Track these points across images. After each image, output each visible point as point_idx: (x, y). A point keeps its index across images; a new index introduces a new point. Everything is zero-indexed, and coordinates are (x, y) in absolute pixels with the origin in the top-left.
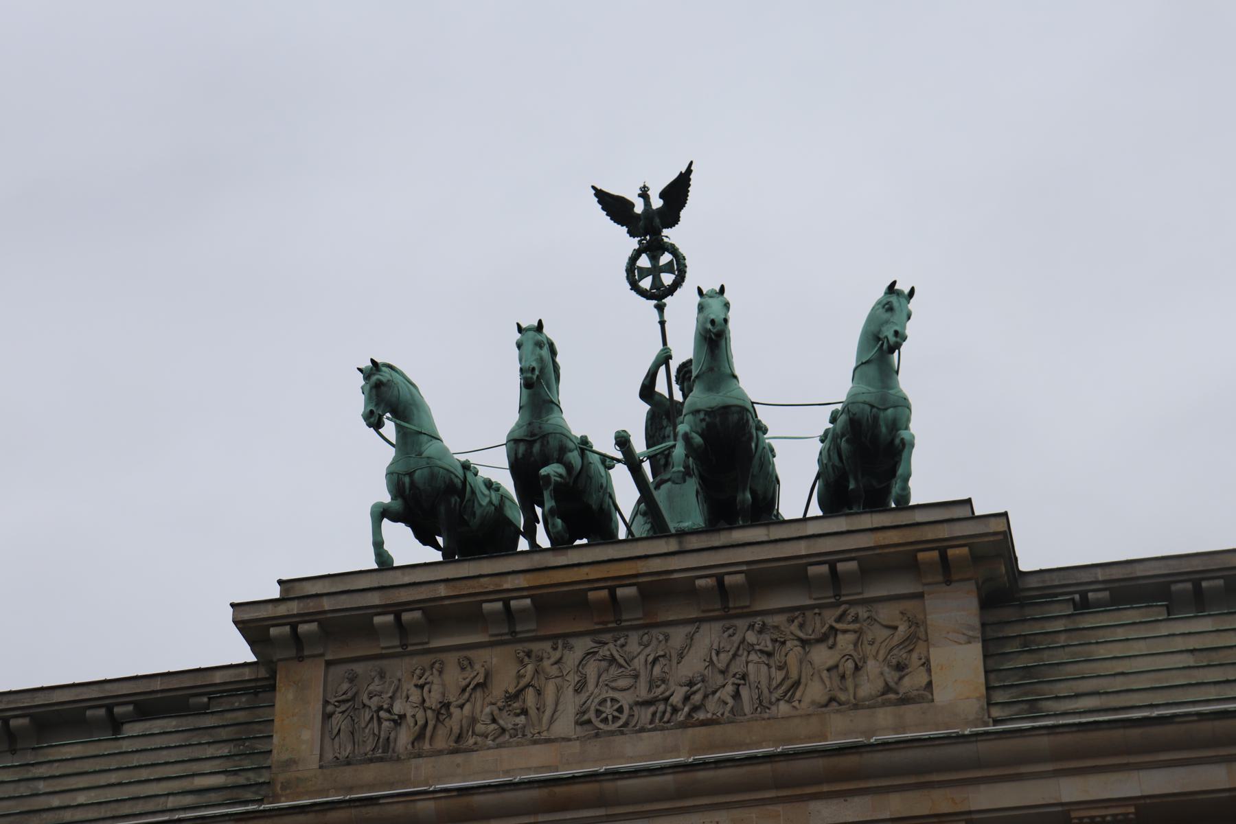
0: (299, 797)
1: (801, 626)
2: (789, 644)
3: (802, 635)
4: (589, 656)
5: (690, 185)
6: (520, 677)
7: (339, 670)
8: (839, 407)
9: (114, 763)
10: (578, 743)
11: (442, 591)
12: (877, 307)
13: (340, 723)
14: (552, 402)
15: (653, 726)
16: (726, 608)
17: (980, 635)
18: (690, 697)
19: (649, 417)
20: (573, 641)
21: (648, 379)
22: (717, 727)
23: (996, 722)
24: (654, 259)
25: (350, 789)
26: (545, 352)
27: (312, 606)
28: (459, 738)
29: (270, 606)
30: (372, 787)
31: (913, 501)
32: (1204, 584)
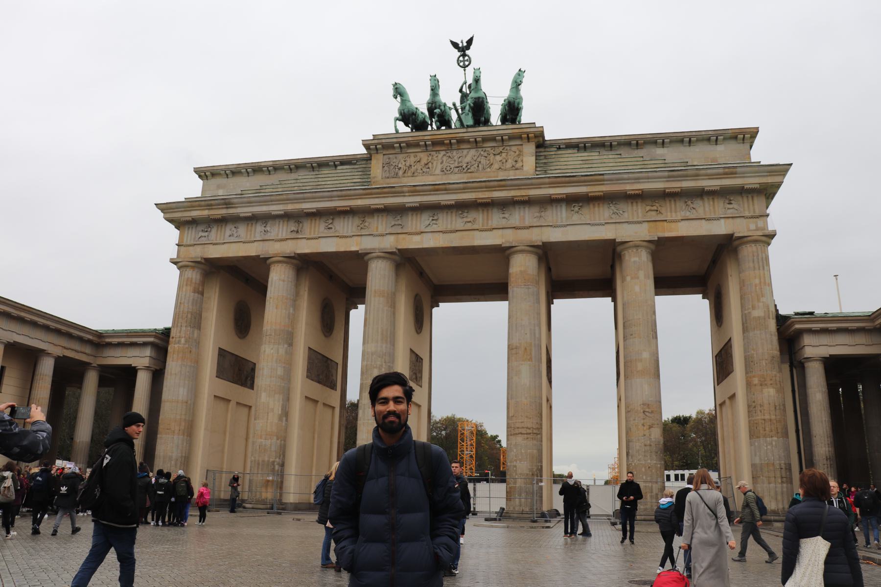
0: (377, 185)
1: (494, 151)
6: (428, 160)
7: (386, 156)
8: (506, 98)
9: (336, 175)
11: (410, 139)
16: (477, 146)
20: (440, 152)
22: (473, 174)
23: (537, 175)
24: (464, 58)
25: (388, 184)
26: (436, 82)
27: (380, 141)
28: (413, 173)
30: (394, 184)
31: (521, 123)
32: (587, 145)
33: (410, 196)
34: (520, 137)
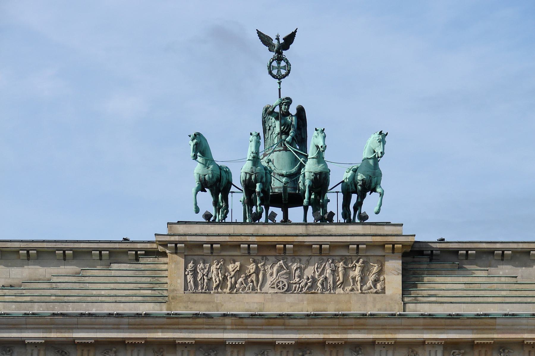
2: (340, 269)
3: (345, 266)
4: (275, 264)
5: (295, 36)
9: (112, 280)
10: (270, 294)
11: (227, 239)
12: (374, 139)
13: (190, 279)
14: (259, 159)
15: (295, 292)
16: (321, 253)
17: (401, 273)
18: (307, 283)
19: (264, 110)
20: (269, 258)
21: (272, 109)
24: (279, 64)
27: (183, 238)
29: (168, 237)
33: (232, 329)
34: (382, 246)
